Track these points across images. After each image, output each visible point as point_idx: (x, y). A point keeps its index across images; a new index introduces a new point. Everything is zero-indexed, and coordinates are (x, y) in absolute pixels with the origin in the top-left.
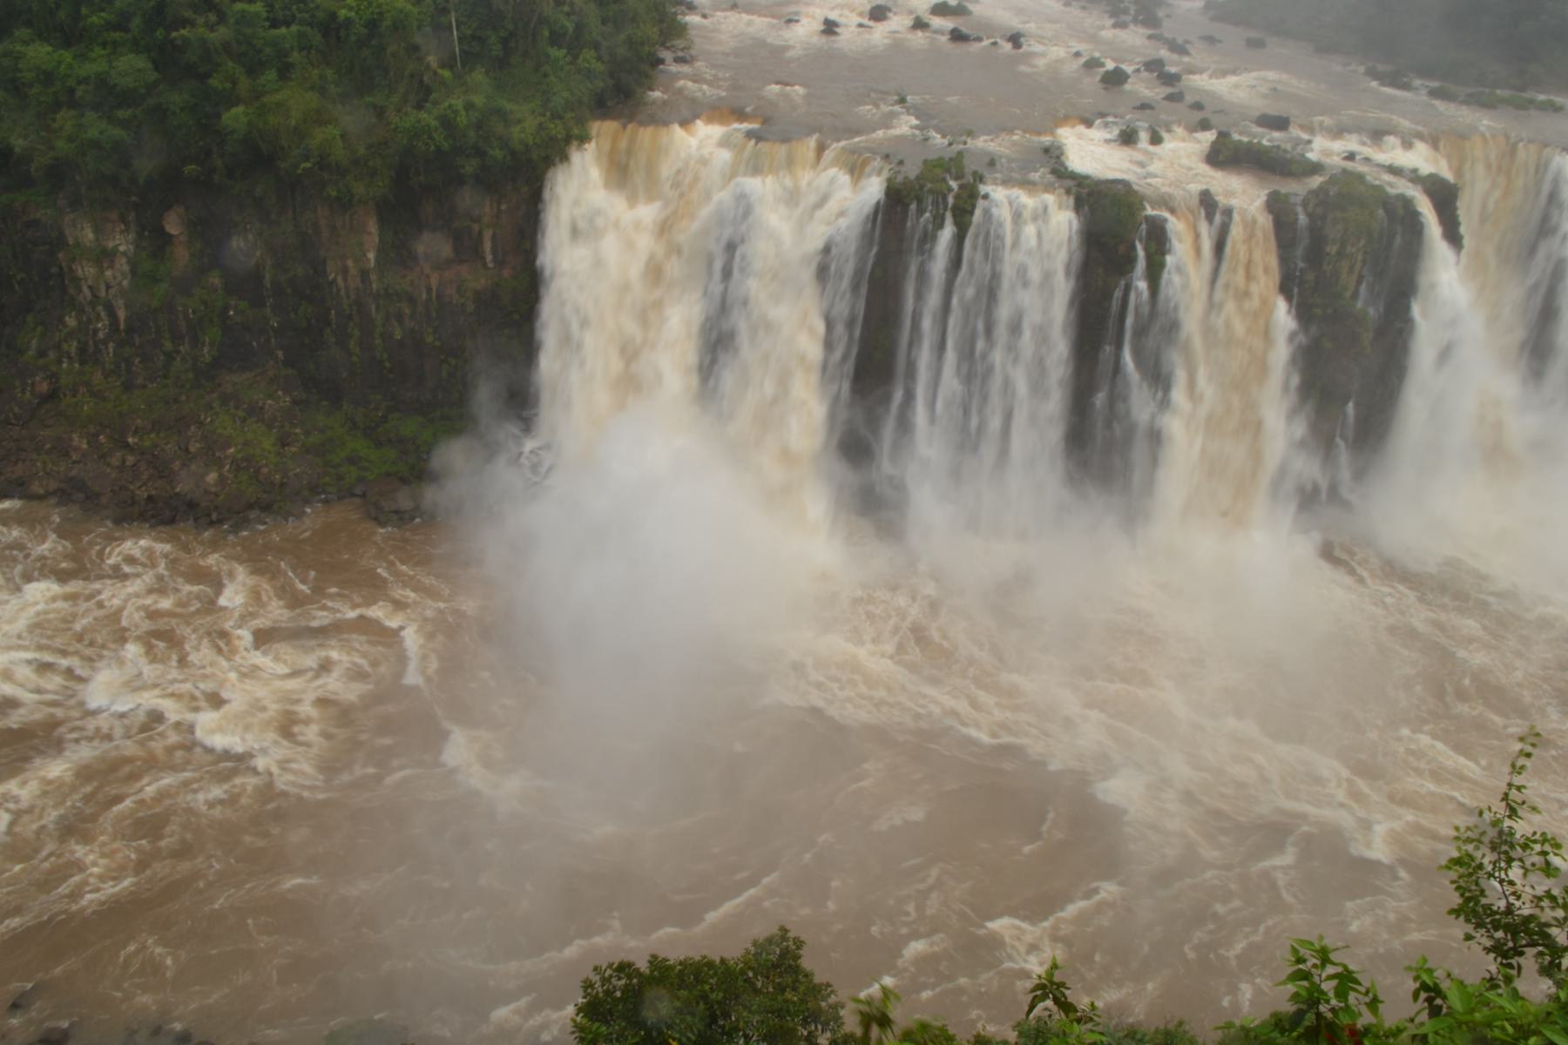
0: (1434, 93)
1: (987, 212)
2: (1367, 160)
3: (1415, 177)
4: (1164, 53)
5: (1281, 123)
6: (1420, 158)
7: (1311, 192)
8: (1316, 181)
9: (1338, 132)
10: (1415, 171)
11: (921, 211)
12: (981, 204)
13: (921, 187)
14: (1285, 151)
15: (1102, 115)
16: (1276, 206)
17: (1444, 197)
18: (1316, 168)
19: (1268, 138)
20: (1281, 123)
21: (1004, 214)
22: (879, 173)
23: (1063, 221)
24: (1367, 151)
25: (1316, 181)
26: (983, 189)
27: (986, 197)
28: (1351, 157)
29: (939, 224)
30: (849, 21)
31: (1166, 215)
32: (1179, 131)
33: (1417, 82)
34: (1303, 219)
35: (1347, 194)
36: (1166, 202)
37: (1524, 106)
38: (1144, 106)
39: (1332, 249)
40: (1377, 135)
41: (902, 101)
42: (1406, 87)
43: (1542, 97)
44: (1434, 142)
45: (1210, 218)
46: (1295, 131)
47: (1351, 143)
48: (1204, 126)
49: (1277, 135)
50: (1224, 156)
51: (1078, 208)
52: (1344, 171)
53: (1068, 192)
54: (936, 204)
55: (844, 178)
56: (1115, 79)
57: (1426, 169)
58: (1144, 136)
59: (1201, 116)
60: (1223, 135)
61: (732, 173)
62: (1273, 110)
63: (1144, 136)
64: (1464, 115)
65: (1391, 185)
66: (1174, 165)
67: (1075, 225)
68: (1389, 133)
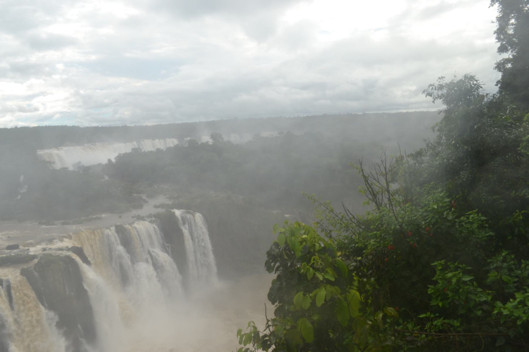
0: (64, 224)
2: (50, 249)
3: (68, 249)
5: (16, 247)
6: (67, 243)
7: (36, 265)
8: (36, 261)
9: (38, 243)
10: (67, 247)
14: (21, 255)
16: (24, 273)
17: (79, 251)
18: (34, 257)
19: (14, 252)
20: (16, 247)
24: (49, 246)
25: (36, 261)
28: (44, 250)
33: (56, 222)
34: (36, 274)
35: (47, 262)
40: (51, 241)
42: (54, 224)
43: (94, 217)
44: (70, 238)
46: (21, 247)
47: (43, 246)
49: (15, 251)
52: (44, 254)
62: (11, 243)
65: (62, 254)
68: (55, 239)
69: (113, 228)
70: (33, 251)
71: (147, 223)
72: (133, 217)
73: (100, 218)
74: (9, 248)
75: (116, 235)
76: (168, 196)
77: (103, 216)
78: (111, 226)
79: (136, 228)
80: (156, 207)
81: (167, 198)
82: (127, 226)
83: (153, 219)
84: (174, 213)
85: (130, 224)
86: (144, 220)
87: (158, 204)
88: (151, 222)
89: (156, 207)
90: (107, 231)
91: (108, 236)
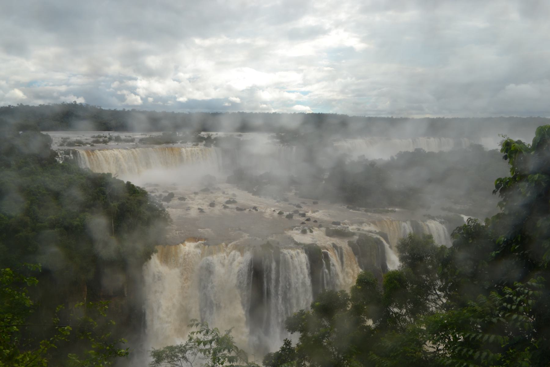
4: (297, 208)
9: (352, 224)
12: (281, 255)
15: (295, 227)
18: (353, 234)
22: (248, 250)
23: (303, 258)
24: (362, 228)
26: (282, 250)
30: (205, 207)
31: (326, 251)
32: (316, 228)
33: (361, 209)
37: (388, 211)
38: (303, 223)
41: (240, 229)
44: (374, 223)
48: (320, 226)
49: (339, 226)
50: (330, 233)
51: (306, 253)
53: (302, 248)
55: (238, 253)
56: (290, 217)
57: (378, 231)
58: (308, 231)
59: (318, 223)
60: (327, 228)
61: (202, 255)
63: (308, 231)
64: (377, 216)
66: (318, 237)
67: (307, 256)
69: (409, 223)
70: (352, 228)
73: (395, 212)
77: (397, 209)
79: (427, 225)
83: (443, 220)
84: (463, 218)
85: (423, 222)
86: (435, 220)
88: (441, 222)
90: (404, 224)
91: (404, 227)
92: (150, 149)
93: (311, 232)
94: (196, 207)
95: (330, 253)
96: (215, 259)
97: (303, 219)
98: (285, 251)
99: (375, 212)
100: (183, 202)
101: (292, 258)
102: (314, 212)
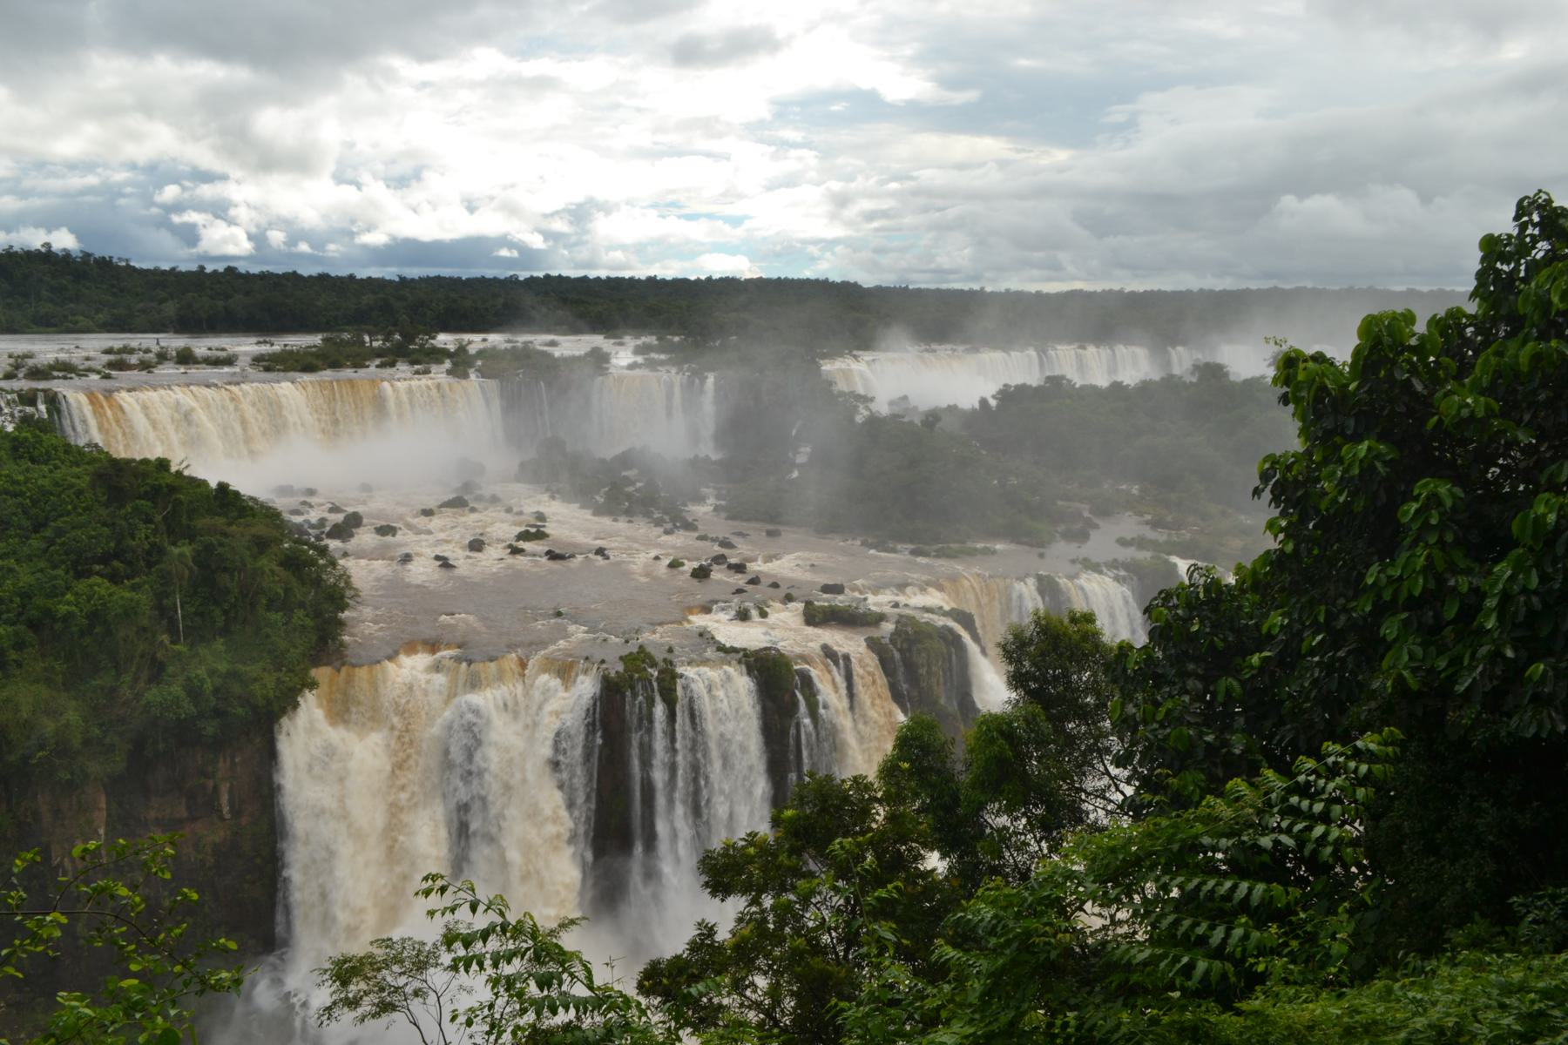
1: (685, 688)
2: (906, 605)
9: (876, 590)
11: (635, 696)
13: (631, 677)
18: (881, 617)
19: (840, 601)
21: (699, 688)
22: (586, 672)
24: (901, 599)
26: (679, 670)
27: (681, 676)
29: (651, 703)
30: (457, 554)
33: (899, 547)
34: (897, 655)
36: (805, 659)
37: (972, 553)
38: (739, 591)
39: (923, 671)
40: (901, 587)
41: (559, 614)
43: (979, 546)
44: (940, 588)
45: (836, 663)
48: (789, 598)
49: (841, 597)
50: (814, 617)
51: (749, 673)
53: (740, 662)
54: (645, 688)
55: (555, 682)
56: (701, 574)
57: (947, 608)
58: (754, 613)
60: (808, 604)
63: (754, 613)
64: (943, 565)
66: (781, 630)
69: (1031, 581)
70: (877, 602)
71: (1107, 580)
72: (1073, 561)
73: (994, 552)
74: (827, 589)
75: (1039, 598)
76: (1149, 517)
77: (999, 547)
78: (1027, 575)
79: (1082, 588)
80: (1123, 542)
81: (1147, 523)
82: (1063, 581)
83: (1122, 573)
84: (1175, 565)
85: (1071, 577)
86: (1101, 572)
87: (1129, 537)
88: (1117, 579)
89: (1123, 542)
90: (1019, 587)
91: (1020, 597)
92: (286, 385)
93: (764, 615)
94: (431, 552)
95: (814, 673)
96: (484, 699)
97: (739, 580)
98: (690, 672)
99: (940, 554)
100: (389, 538)
101: (710, 689)
102: (769, 559)
